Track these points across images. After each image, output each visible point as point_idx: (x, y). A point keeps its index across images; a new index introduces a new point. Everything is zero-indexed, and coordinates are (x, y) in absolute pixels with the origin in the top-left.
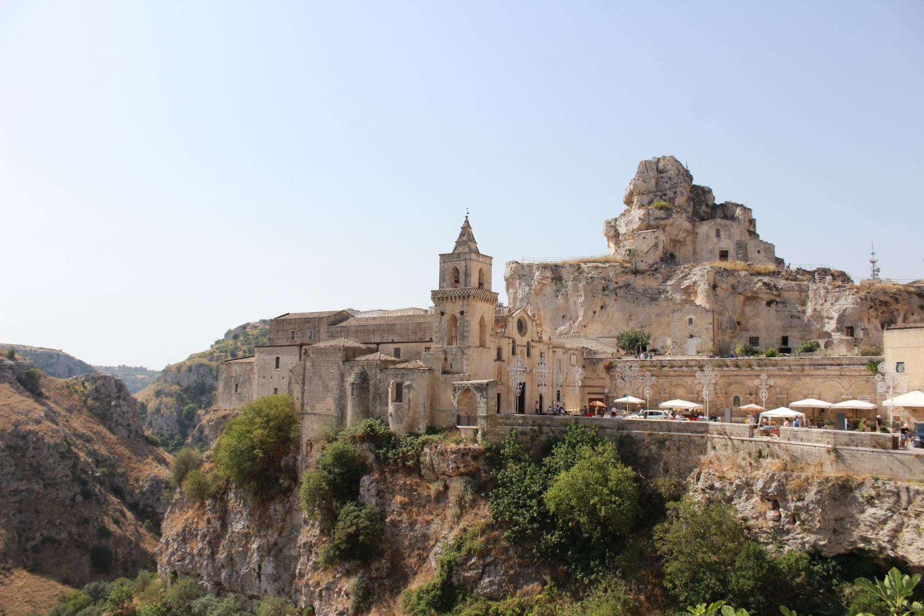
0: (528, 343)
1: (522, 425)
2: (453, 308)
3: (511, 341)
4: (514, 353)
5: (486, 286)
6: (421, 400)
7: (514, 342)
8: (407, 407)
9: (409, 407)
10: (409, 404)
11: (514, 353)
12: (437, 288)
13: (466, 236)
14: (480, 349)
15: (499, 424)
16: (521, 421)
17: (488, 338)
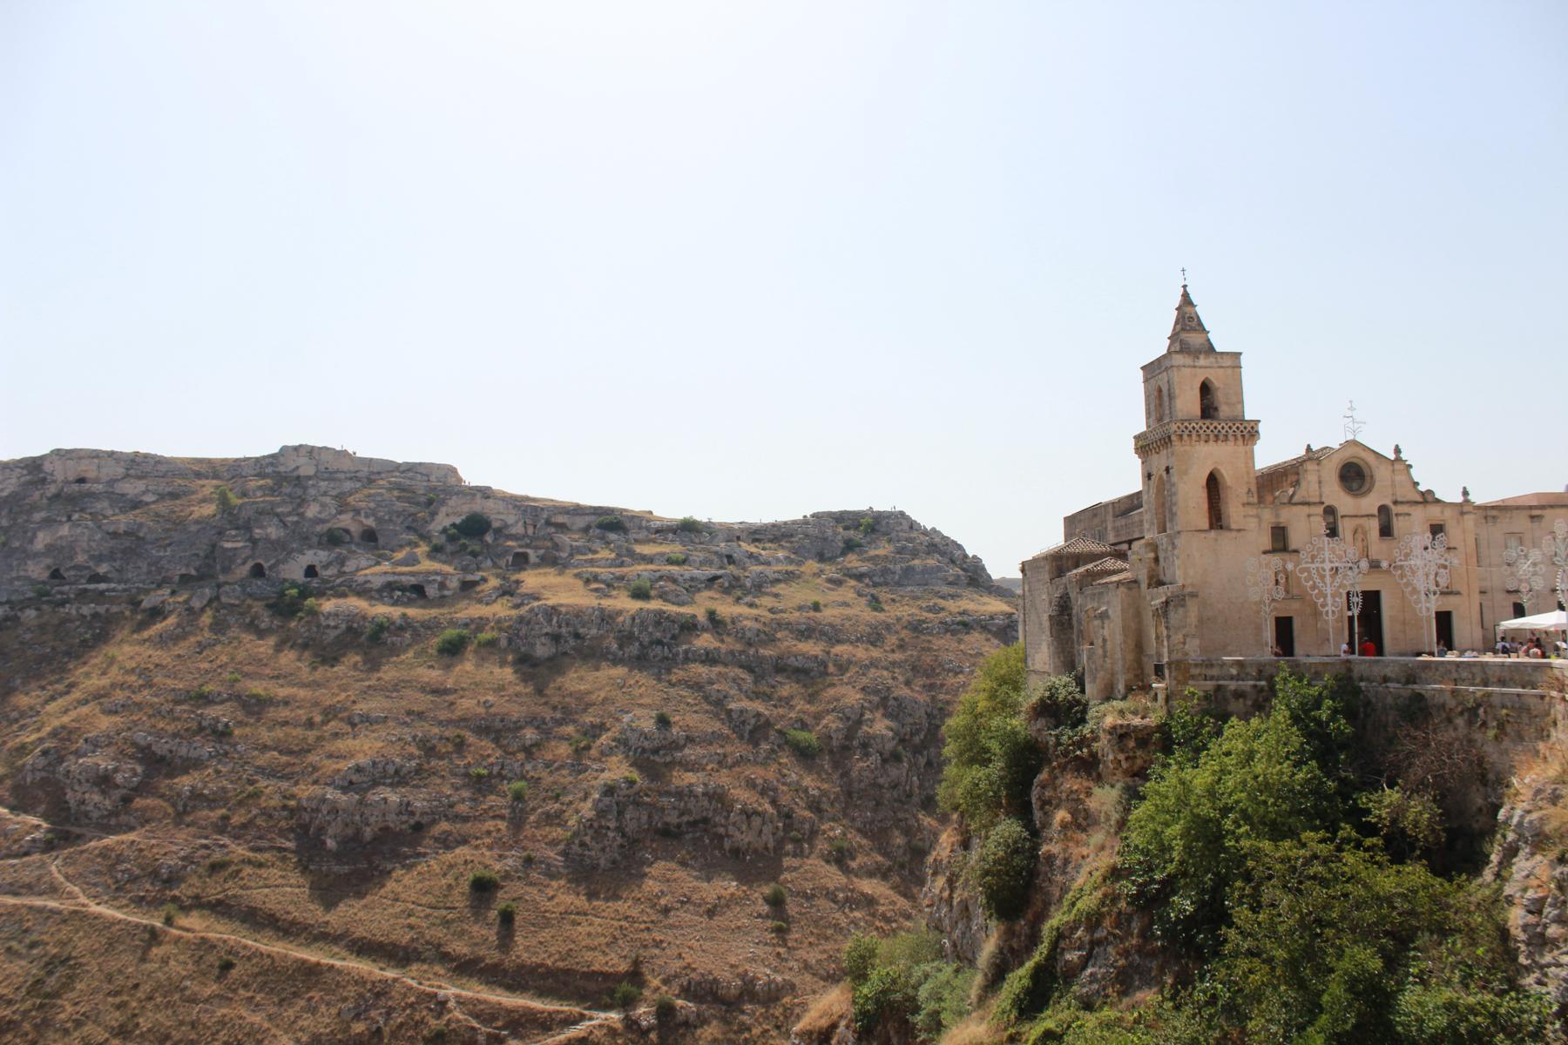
0: (1383, 510)
1: (1237, 678)
2: (1159, 461)
3: (1320, 510)
4: (1333, 532)
5: (1224, 411)
6: (1119, 638)
7: (1330, 511)
8: (1100, 652)
9: (1105, 652)
10: (1104, 646)
11: (1333, 532)
12: (1144, 429)
13: (1187, 320)
14: (1213, 534)
15: (1193, 677)
16: (1234, 671)
17: (1234, 510)
